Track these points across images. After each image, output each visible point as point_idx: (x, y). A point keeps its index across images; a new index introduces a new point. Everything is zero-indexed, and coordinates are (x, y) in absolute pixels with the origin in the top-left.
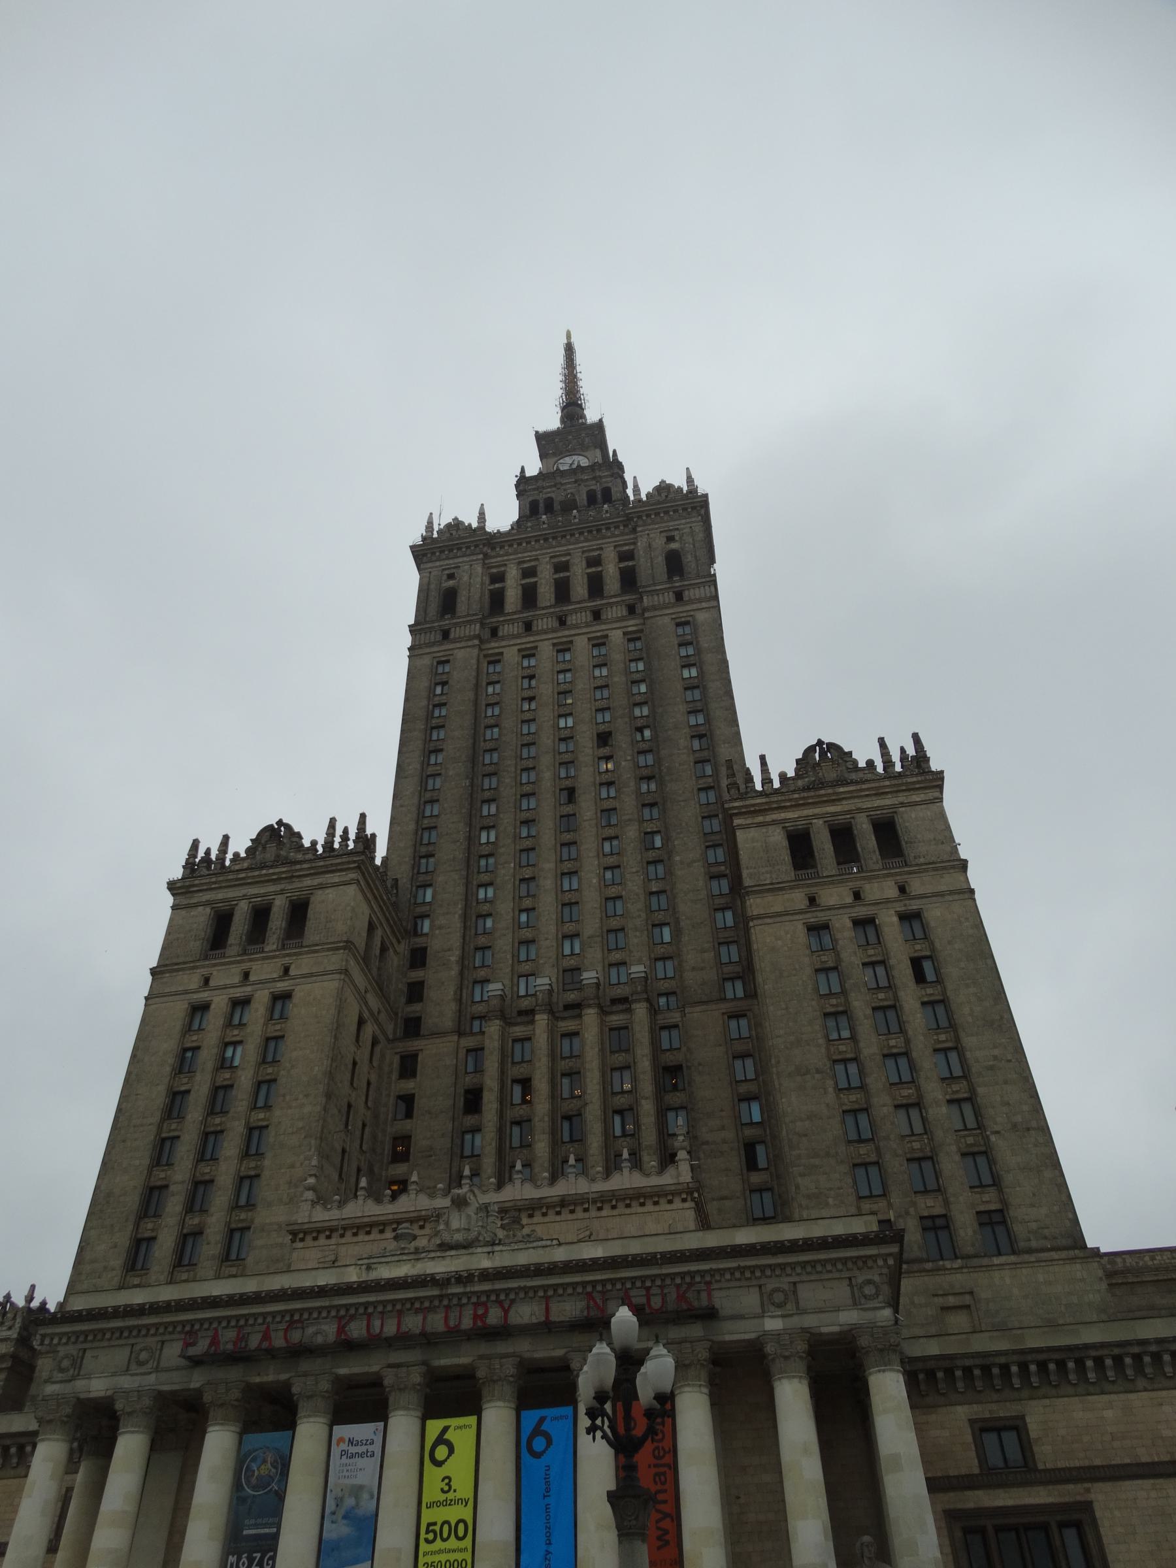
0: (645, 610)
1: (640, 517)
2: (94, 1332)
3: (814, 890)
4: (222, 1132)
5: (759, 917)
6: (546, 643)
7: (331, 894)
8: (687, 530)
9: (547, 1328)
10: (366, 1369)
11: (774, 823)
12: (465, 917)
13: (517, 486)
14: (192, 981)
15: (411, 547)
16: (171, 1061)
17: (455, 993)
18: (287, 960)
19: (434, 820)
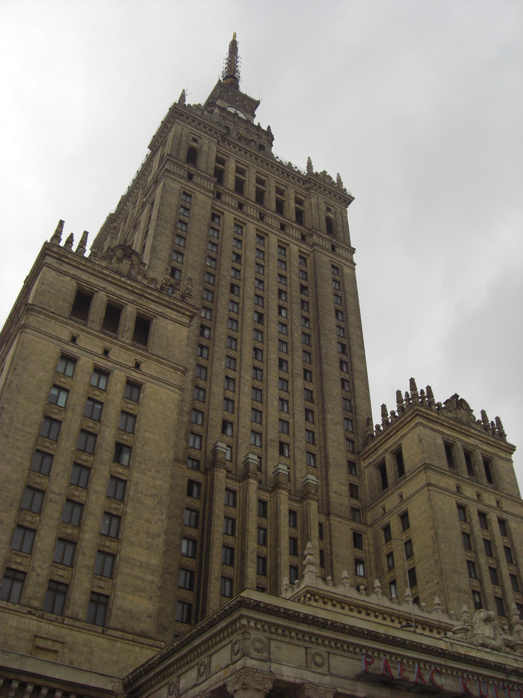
1: (315, 185)
2: (285, 628)
3: (459, 483)
8: (339, 211)
11: (438, 431)
14: (65, 334)
18: (139, 357)
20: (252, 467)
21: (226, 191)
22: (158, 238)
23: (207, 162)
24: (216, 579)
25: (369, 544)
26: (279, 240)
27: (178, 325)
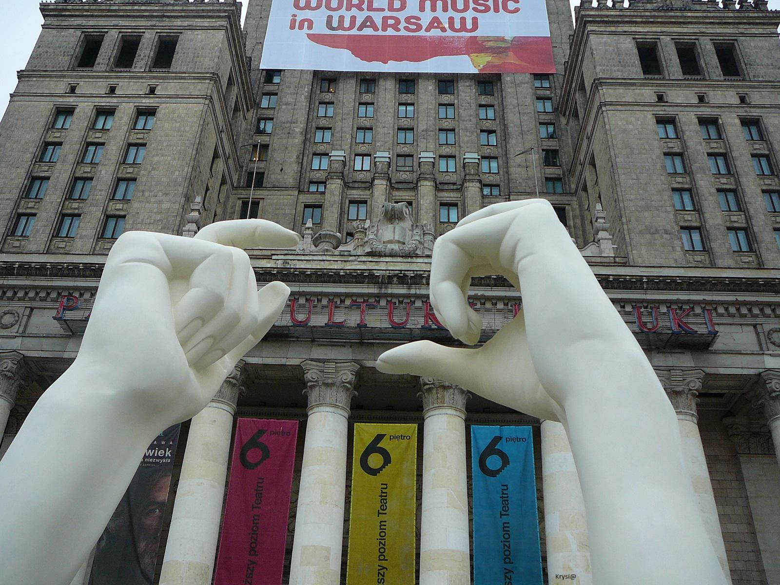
3: (662, 89)
4: (79, 215)
5: (611, 104)
7: (200, 35)
10: (283, 361)
11: (625, 33)
14: (61, 87)
16: (32, 149)
17: (298, 157)
18: (153, 82)
20: (380, 166)
25: (574, 217)
27: (212, 31)
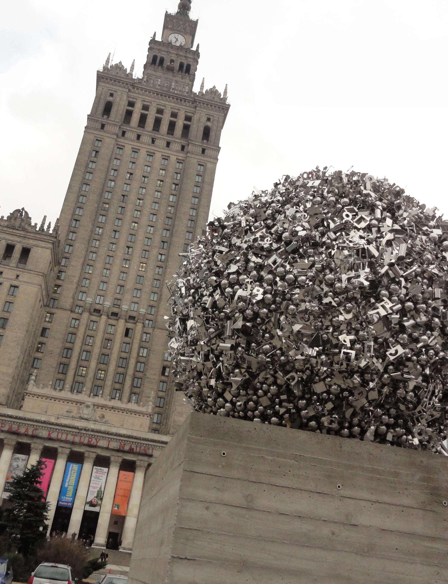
0: (188, 152)
6: (144, 149)
7: (40, 250)
8: (216, 119)
9: (107, 448)
12: (83, 264)
13: (150, 43)
15: (98, 72)
18: (18, 273)
19: (79, 217)
21: (128, 129)
22: (74, 178)
23: (117, 111)
24: (72, 369)
26: (162, 155)
